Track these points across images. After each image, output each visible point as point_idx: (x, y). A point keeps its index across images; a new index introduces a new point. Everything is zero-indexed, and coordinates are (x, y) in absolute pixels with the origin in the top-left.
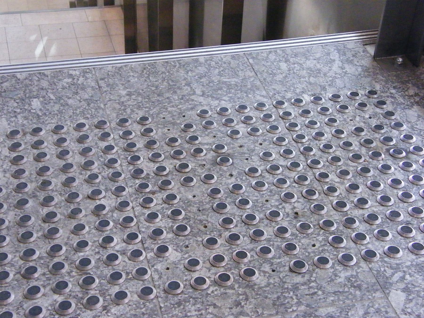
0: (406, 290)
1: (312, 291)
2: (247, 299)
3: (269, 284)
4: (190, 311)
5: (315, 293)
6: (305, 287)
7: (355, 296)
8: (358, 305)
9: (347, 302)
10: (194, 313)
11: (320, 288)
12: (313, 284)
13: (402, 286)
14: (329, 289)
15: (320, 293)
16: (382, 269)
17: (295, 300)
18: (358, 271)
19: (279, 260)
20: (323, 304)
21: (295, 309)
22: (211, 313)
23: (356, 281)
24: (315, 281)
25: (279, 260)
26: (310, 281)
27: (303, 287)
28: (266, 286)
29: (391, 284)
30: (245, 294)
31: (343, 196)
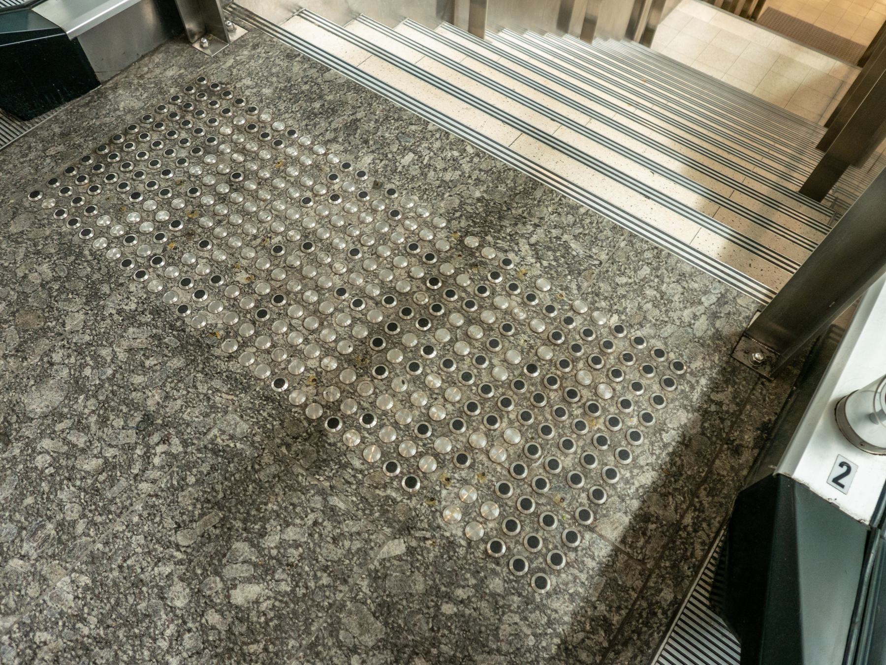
0: (410, 551)
1: (352, 480)
2: (305, 440)
3: (335, 444)
4: (264, 411)
5: (352, 484)
6: (352, 473)
7: (371, 514)
8: (363, 522)
9: (360, 512)
10: (265, 414)
11: (360, 483)
12: (360, 476)
13: (414, 543)
14: (364, 491)
15: (354, 487)
16: (422, 518)
17: (331, 474)
18: (405, 501)
19: (367, 435)
20: (343, 497)
21: (322, 479)
22: (273, 426)
23: (390, 506)
24: (365, 476)
25: (367, 435)
26: (361, 472)
27: (350, 471)
28: (330, 444)
29: (410, 534)
30: (310, 435)
31: (494, 434)
